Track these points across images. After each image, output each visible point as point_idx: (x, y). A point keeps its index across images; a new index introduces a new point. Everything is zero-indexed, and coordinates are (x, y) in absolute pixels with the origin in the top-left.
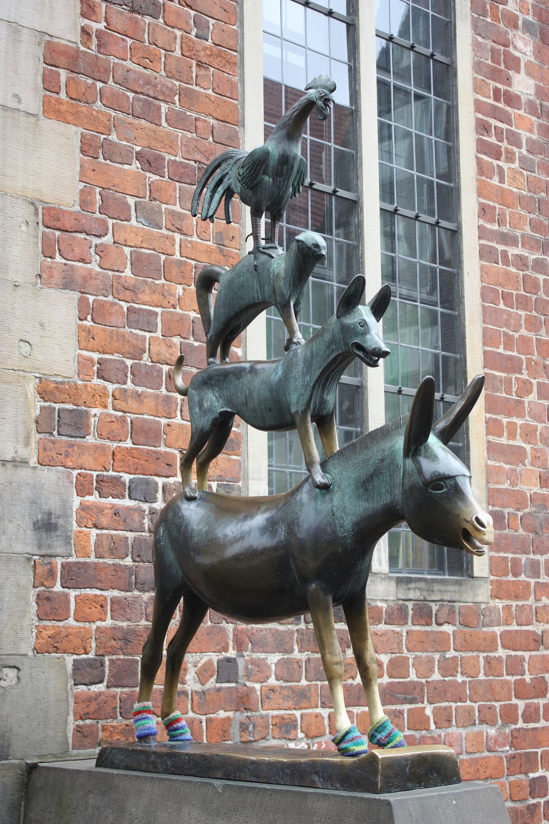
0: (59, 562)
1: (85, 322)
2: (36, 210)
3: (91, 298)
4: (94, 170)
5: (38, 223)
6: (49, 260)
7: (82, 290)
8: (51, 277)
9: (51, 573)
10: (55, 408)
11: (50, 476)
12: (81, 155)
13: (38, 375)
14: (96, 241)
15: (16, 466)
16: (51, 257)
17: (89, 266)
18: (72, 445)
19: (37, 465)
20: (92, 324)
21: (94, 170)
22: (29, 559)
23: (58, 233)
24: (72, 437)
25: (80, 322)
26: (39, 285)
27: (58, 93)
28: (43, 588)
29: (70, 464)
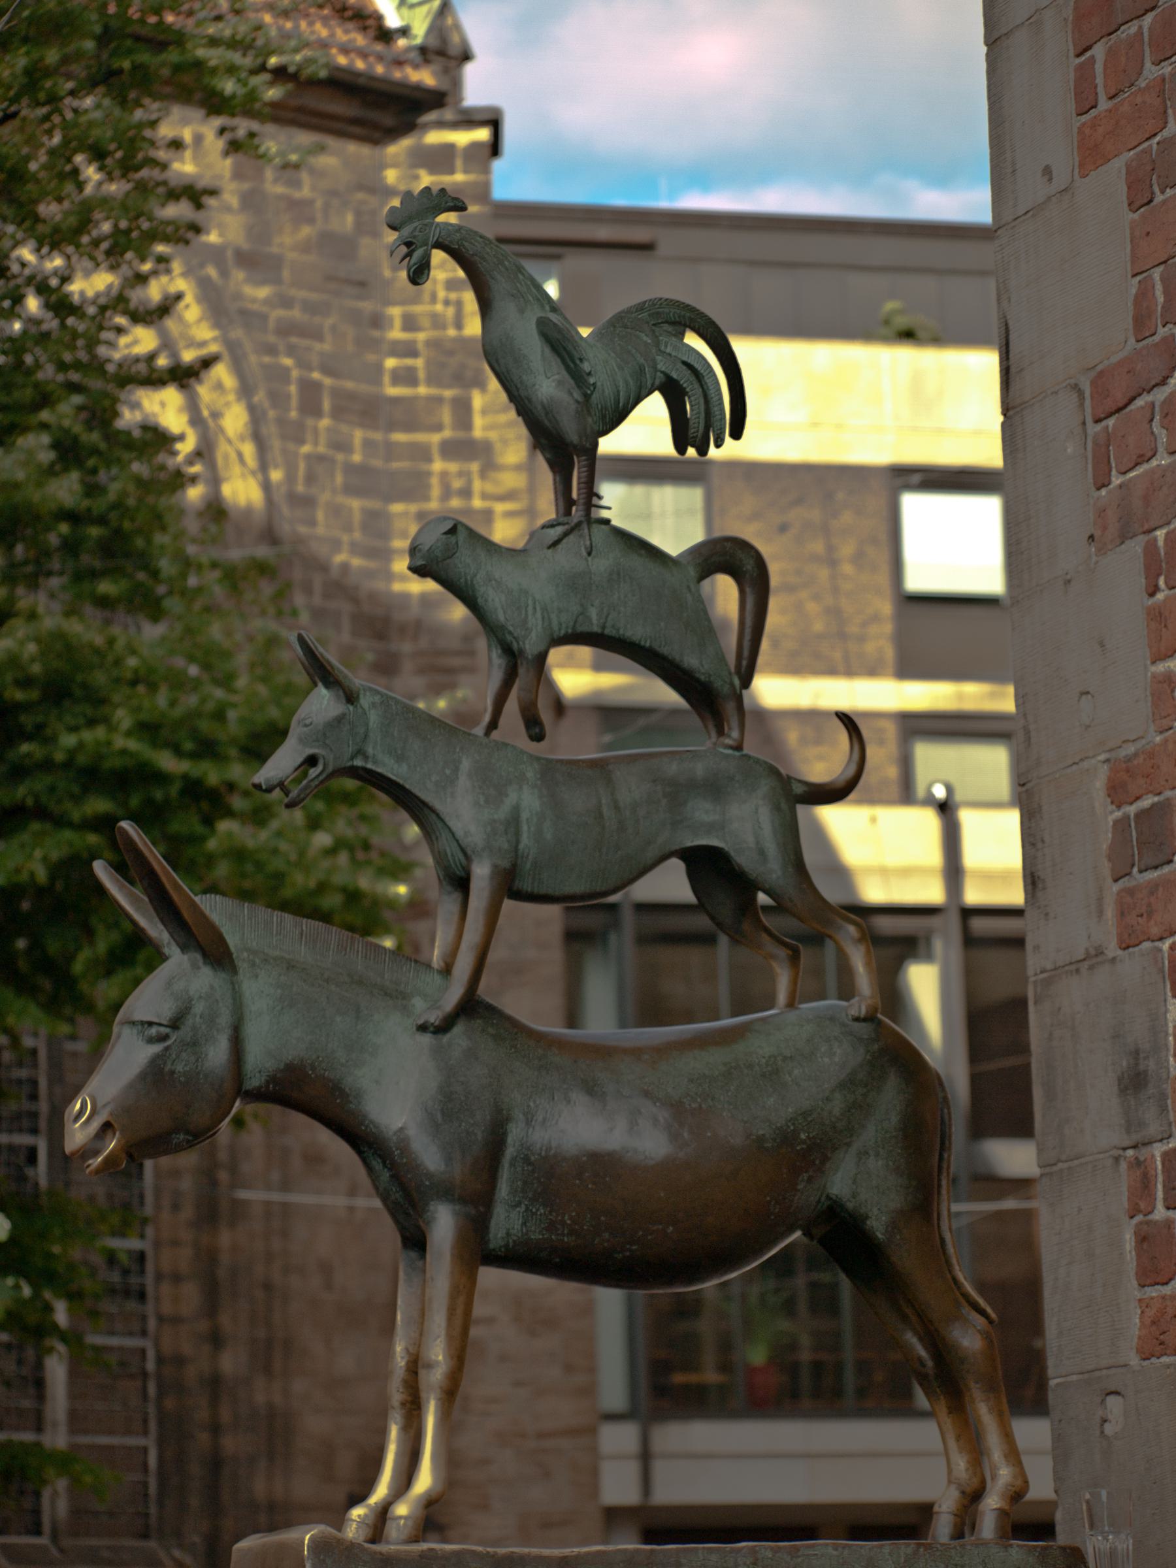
0: (1158, 1150)
1: (1160, 596)
2: (1081, 393)
3: (1160, 534)
4: (1148, 234)
5: (1084, 423)
6: (1103, 492)
7: (1146, 527)
8: (1104, 528)
9: (1145, 1185)
10: (1128, 817)
11: (1133, 967)
12: (1131, 215)
13: (1102, 757)
14: (1160, 395)
15: (1091, 968)
16: (1104, 486)
17: (1154, 463)
18: (1153, 888)
19: (1120, 952)
20: (1167, 592)
21: (1148, 234)
22: (1117, 1159)
23: (1111, 422)
24: (1156, 867)
25: (1151, 601)
26: (1094, 559)
27: (1094, 107)
28: (1139, 1218)
29: (1155, 931)
